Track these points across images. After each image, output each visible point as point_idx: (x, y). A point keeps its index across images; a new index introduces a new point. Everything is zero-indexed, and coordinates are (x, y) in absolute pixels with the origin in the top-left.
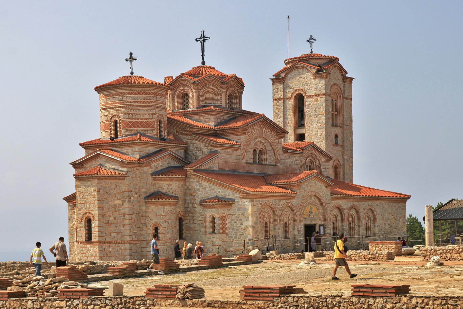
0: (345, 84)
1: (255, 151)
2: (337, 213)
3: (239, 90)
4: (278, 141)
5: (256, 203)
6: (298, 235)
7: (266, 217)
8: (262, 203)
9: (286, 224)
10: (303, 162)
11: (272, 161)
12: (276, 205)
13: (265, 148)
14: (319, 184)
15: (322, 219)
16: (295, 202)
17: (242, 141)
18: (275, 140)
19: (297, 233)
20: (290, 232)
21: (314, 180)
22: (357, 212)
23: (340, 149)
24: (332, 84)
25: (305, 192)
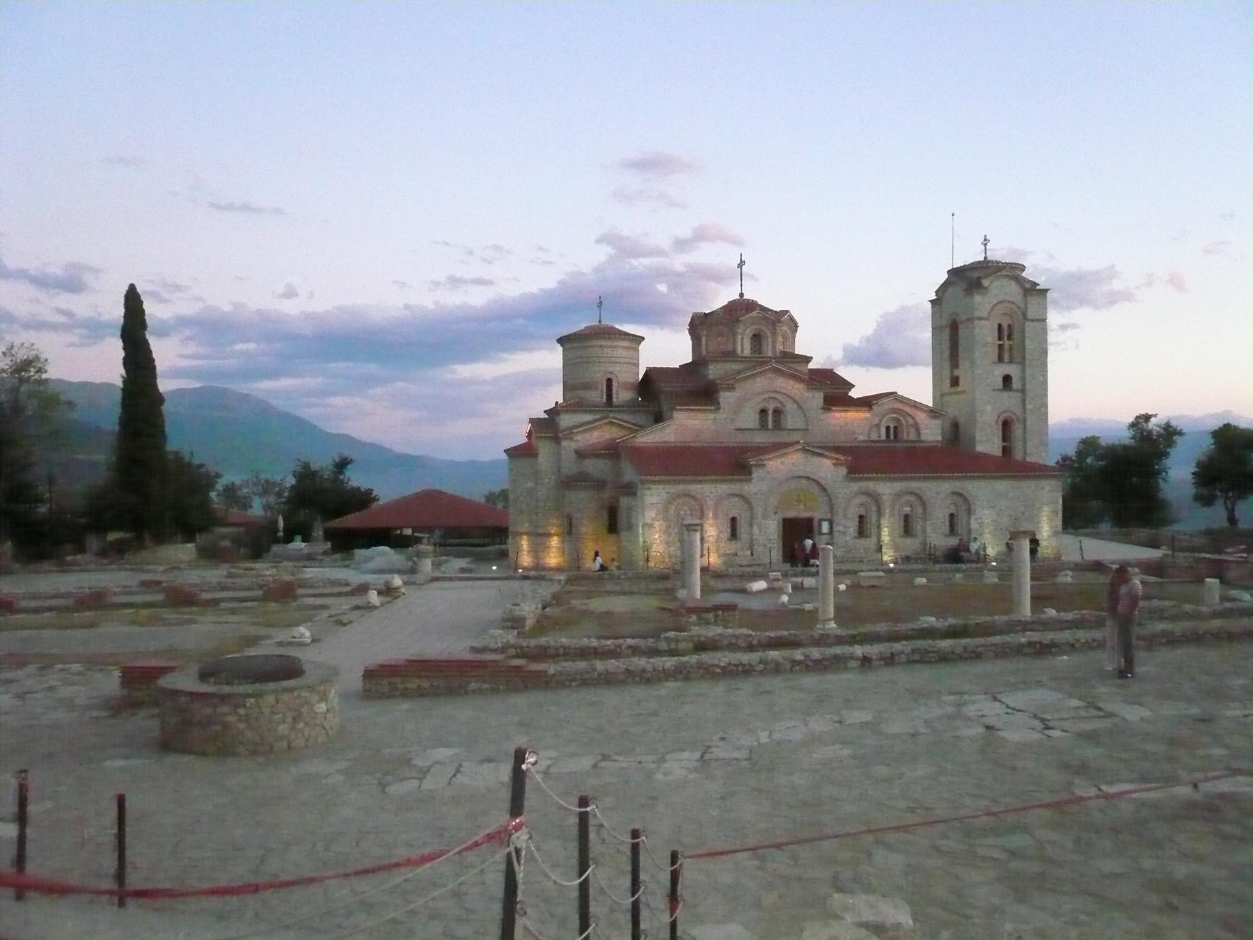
1: (763, 412)
4: (813, 396)
6: (758, 535)
7: (685, 511)
9: (734, 520)
10: (877, 420)
12: (704, 493)
13: (784, 406)
16: (749, 489)
20: (743, 530)
22: (919, 497)
23: (1019, 394)
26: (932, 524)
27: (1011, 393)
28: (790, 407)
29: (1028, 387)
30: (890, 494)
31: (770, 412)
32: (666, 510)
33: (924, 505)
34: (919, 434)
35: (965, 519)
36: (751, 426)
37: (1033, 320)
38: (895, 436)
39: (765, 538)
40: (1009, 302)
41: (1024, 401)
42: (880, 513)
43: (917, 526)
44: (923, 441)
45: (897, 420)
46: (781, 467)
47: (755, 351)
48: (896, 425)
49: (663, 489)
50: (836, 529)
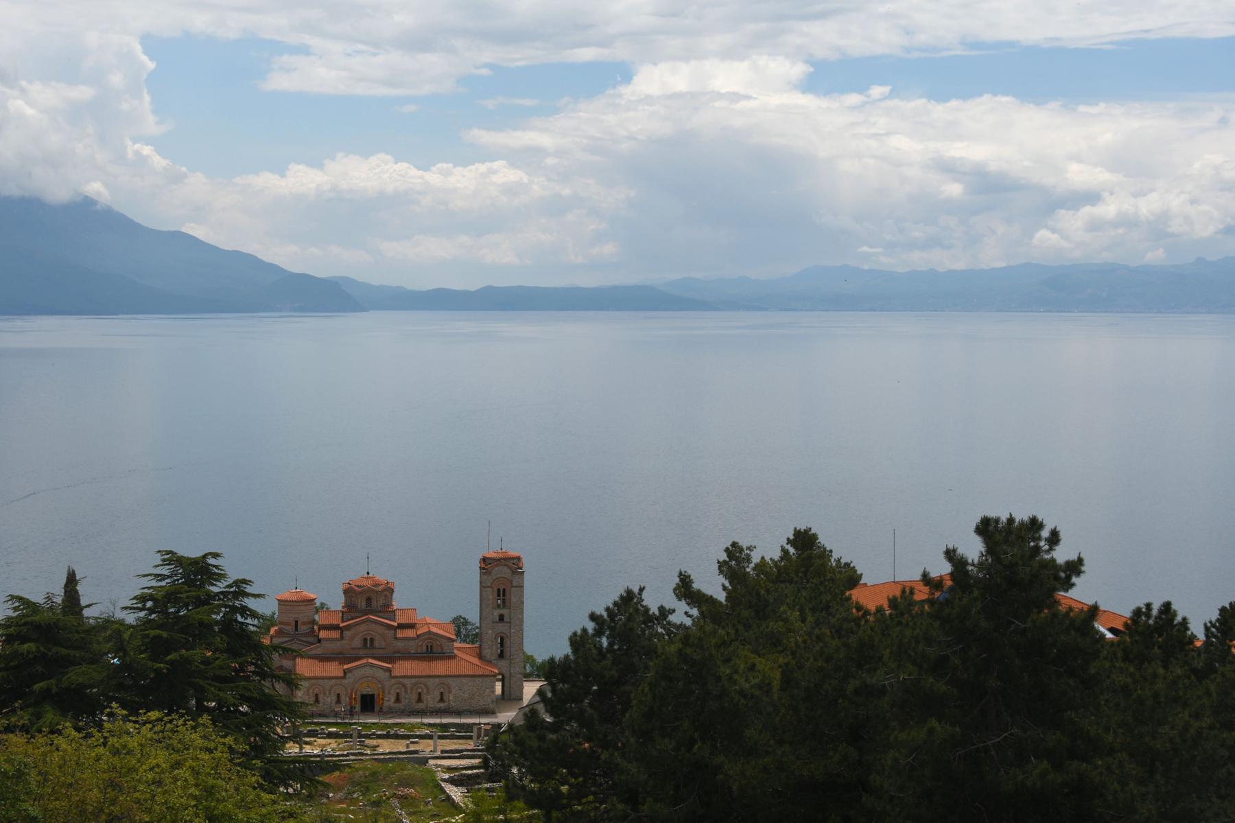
1: (365, 640)
9: (338, 694)
10: (420, 643)
14: (375, 669)
23: (508, 624)
27: (503, 624)
29: (512, 621)
31: (369, 640)
32: (308, 691)
34: (442, 649)
35: (447, 694)
36: (359, 646)
37: (516, 587)
41: (510, 627)
42: (406, 692)
43: (424, 697)
44: (444, 653)
45: (431, 642)
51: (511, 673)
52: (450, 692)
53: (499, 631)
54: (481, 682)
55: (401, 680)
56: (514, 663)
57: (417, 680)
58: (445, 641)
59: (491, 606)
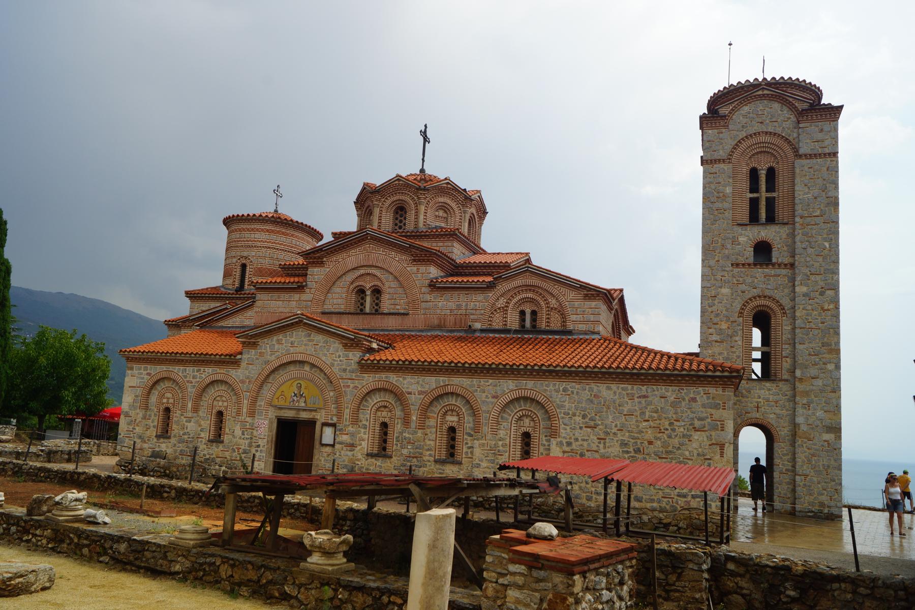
0: (801, 125)
1: (361, 292)
2: (393, 403)
3: (416, 198)
4: (418, 269)
5: (137, 372)
6: (240, 438)
7: (168, 398)
8: (152, 372)
10: (501, 302)
11: (398, 307)
12: (186, 377)
14: (319, 338)
15: (335, 412)
17: (316, 277)
18: (408, 269)
19: (240, 433)
20: (227, 430)
21: (302, 331)
22: (468, 402)
23: (784, 272)
24: (743, 134)
25: (271, 355)
26: (483, 445)
28: (389, 286)
30: (420, 393)
33: (474, 412)
36: (342, 308)
38: (534, 326)
39: (247, 442)
40: (766, 133)
41: (793, 280)
42: (406, 422)
44: (570, 332)
45: (532, 301)
46: (277, 346)
47: (400, 228)
48: (535, 308)
49: (146, 369)
50: (337, 440)
51: (795, 426)
52: (553, 433)
53: (755, 292)
54: (674, 405)
55: (394, 378)
56: (806, 394)
57: (442, 380)
58: (572, 295)
59: (728, 214)
